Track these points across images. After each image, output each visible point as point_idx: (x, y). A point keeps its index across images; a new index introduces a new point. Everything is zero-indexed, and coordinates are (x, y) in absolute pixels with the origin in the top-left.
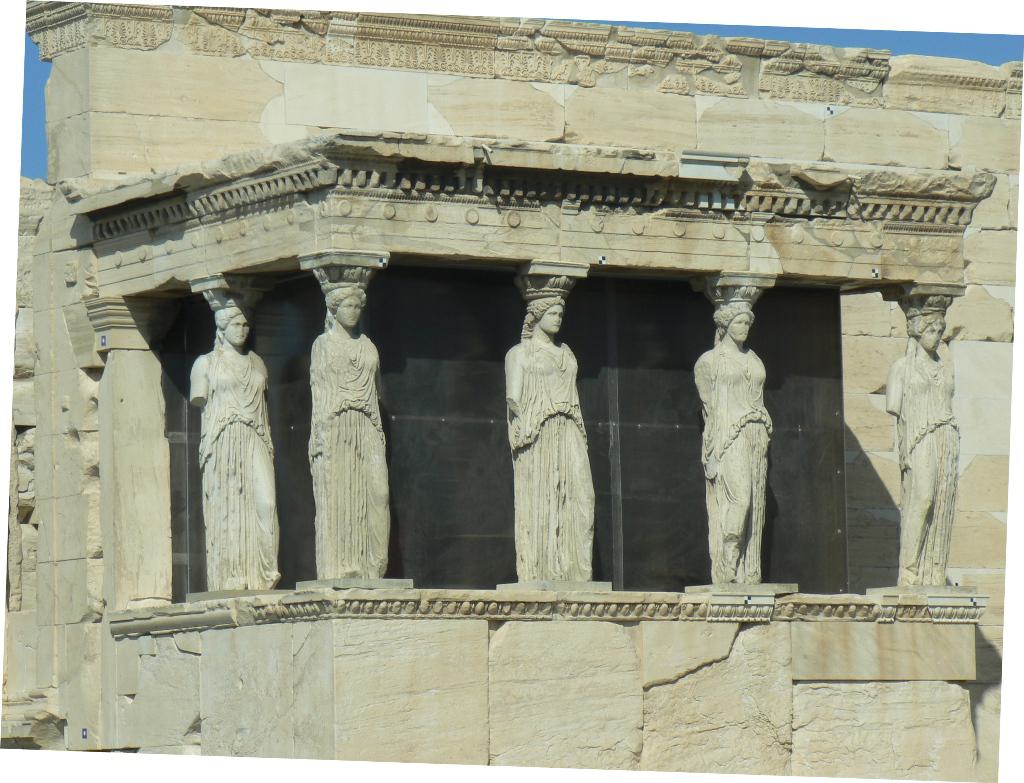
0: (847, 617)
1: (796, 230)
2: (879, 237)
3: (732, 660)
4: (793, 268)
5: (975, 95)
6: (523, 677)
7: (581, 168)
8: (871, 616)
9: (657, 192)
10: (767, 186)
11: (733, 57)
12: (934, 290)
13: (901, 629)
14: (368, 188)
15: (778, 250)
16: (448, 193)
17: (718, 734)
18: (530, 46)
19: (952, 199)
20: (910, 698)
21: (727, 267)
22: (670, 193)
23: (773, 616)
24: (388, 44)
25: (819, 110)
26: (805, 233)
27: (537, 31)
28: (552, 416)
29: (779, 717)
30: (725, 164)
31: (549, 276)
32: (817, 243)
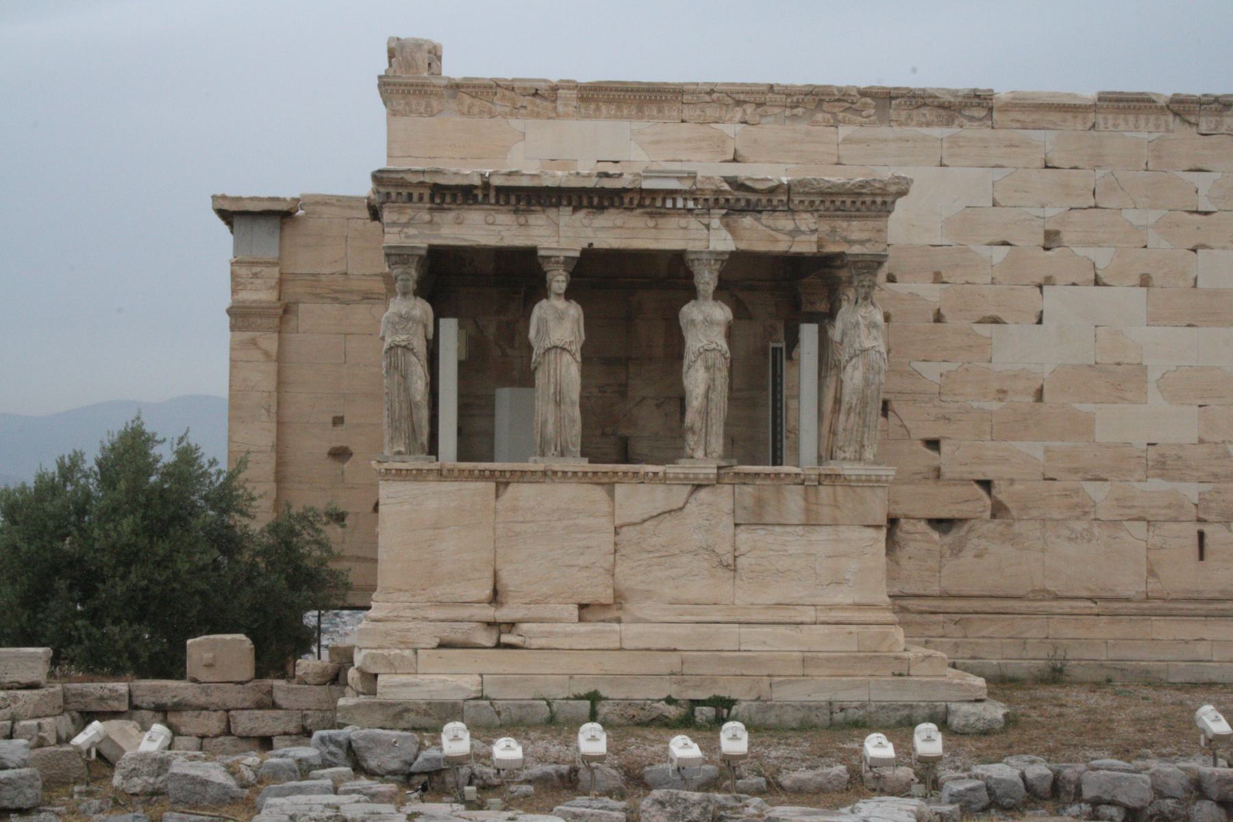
1: (747, 221)
3: (686, 510)
4: (743, 246)
5: (1069, 116)
6: (521, 519)
7: (563, 185)
8: (798, 481)
9: (631, 199)
10: (719, 192)
11: (869, 100)
12: (860, 258)
13: (825, 491)
19: (873, 194)
21: (691, 246)
22: (642, 198)
23: (719, 479)
25: (937, 132)
26: (756, 224)
28: (549, 349)
29: (724, 549)
30: (678, 178)
31: (549, 257)
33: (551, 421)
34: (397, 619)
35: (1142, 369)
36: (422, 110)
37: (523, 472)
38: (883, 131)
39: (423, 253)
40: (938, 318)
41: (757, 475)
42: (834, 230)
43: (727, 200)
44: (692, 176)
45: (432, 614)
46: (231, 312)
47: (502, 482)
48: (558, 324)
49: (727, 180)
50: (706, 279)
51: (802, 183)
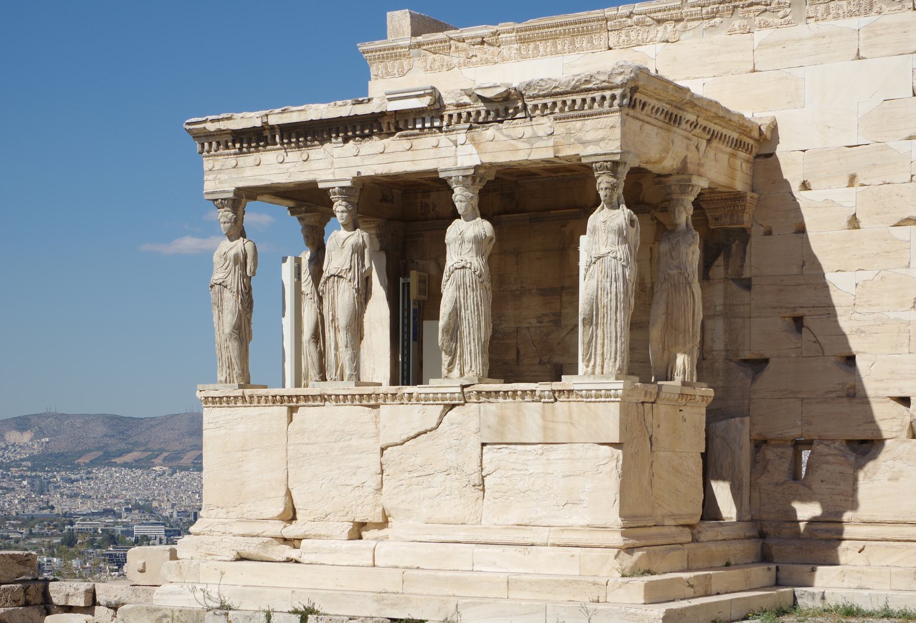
0: (519, 399)
1: (490, 132)
2: (550, 127)
4: (487, 159)
10: (459, 105)
14: (213, 152)
15: (477, 148)
16: (263, 146)
17: (430, 478)
18: (630, 24)
20: (567, 456)
22: (397, 122)
24: (538, 43)
25: (854, 23)
27: (632, 13)
28: (329, 278)
32: (505, 138)
33: (333, 346)
36: (395, 71)
37: (306, 398)
38: (801, 30)
39: (231, 195)
41: (497, 392)
42: (569, 133)
43: (469, 114)
47: (293, 404)
50: (461, 197)
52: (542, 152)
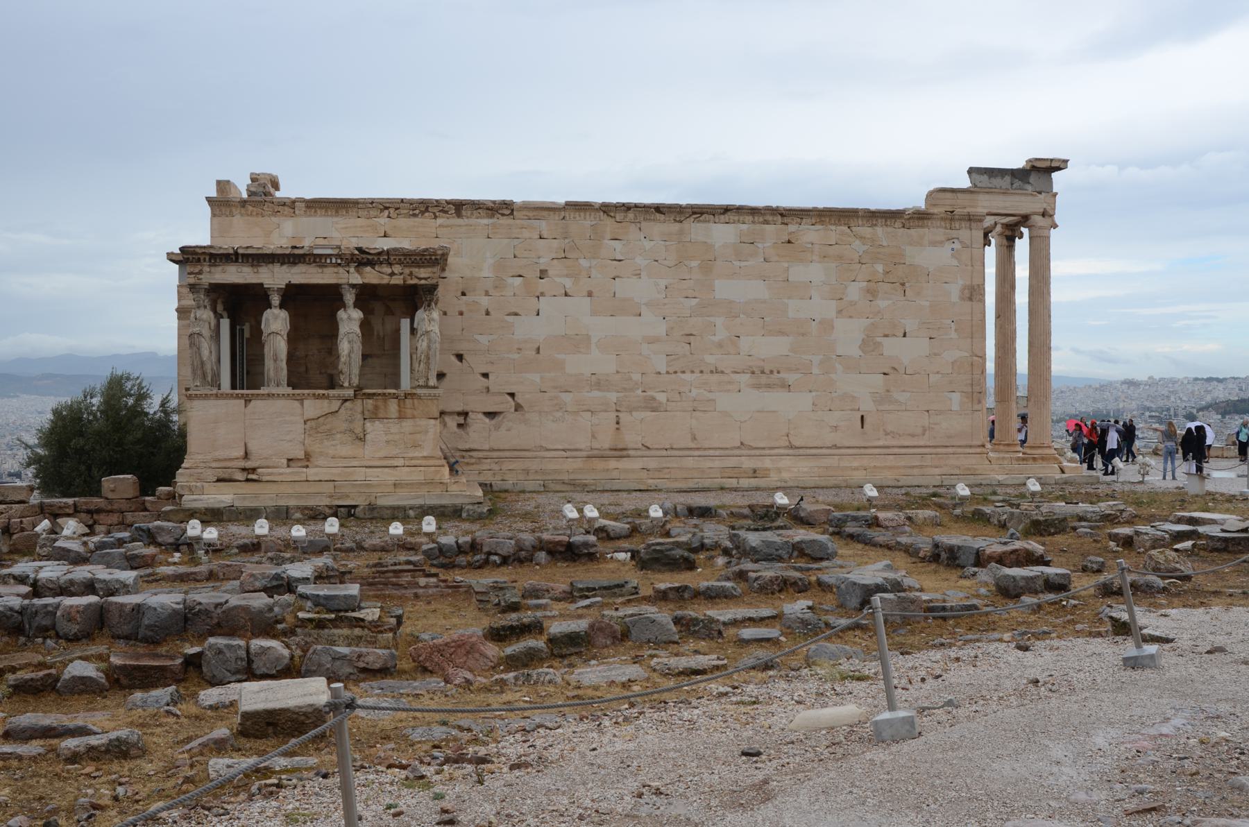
1: (368, 269)
4: (366, 281)
10: (353, 255)
21: (340, 281)
25: (486, 221)
29: (358, 430)
34: (197, 467)
35: (588, 338)
38: (459, 221)
40: (488, 313)
41: (374, 394)
44: (339, 247)
45: (214, 465)
46: (177, 310)
48: (276, 322)
49: (357, 249)
51: (395, 250)
52: (397, 280)
